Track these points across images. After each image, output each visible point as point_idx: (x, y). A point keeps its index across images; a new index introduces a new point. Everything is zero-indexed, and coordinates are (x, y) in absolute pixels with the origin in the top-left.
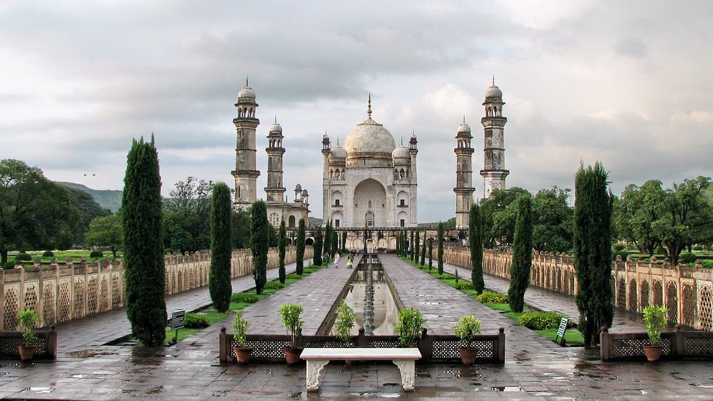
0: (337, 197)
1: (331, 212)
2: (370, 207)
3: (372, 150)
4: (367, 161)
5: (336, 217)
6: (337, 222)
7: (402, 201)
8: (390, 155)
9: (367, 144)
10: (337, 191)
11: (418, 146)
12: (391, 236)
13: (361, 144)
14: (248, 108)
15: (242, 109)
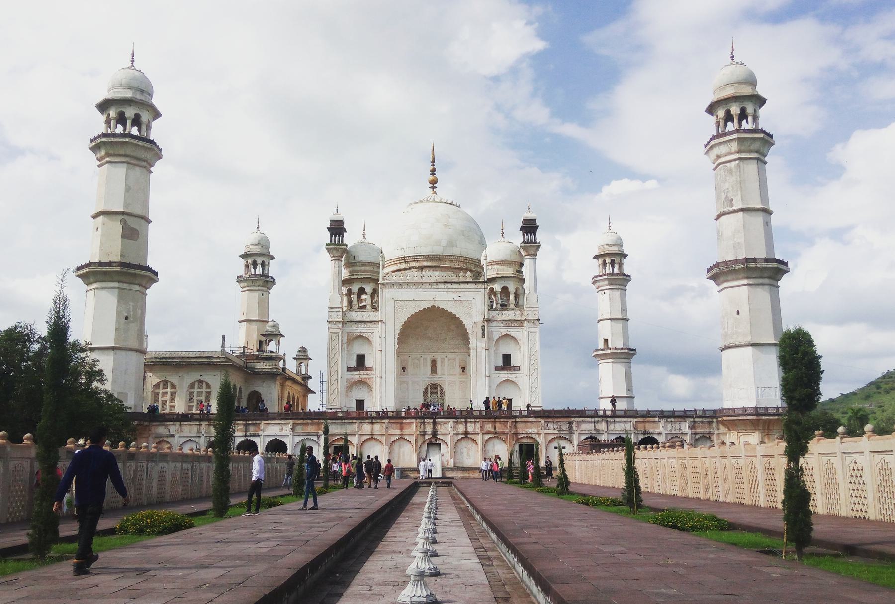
0: (359, 349)
2: (434, 370)
3: (438, 250)
4: (426, 273)
5: (359, 394)
7: (507, 358)
8: (477, 263)
10: (360, 336)
11: (540, 236)
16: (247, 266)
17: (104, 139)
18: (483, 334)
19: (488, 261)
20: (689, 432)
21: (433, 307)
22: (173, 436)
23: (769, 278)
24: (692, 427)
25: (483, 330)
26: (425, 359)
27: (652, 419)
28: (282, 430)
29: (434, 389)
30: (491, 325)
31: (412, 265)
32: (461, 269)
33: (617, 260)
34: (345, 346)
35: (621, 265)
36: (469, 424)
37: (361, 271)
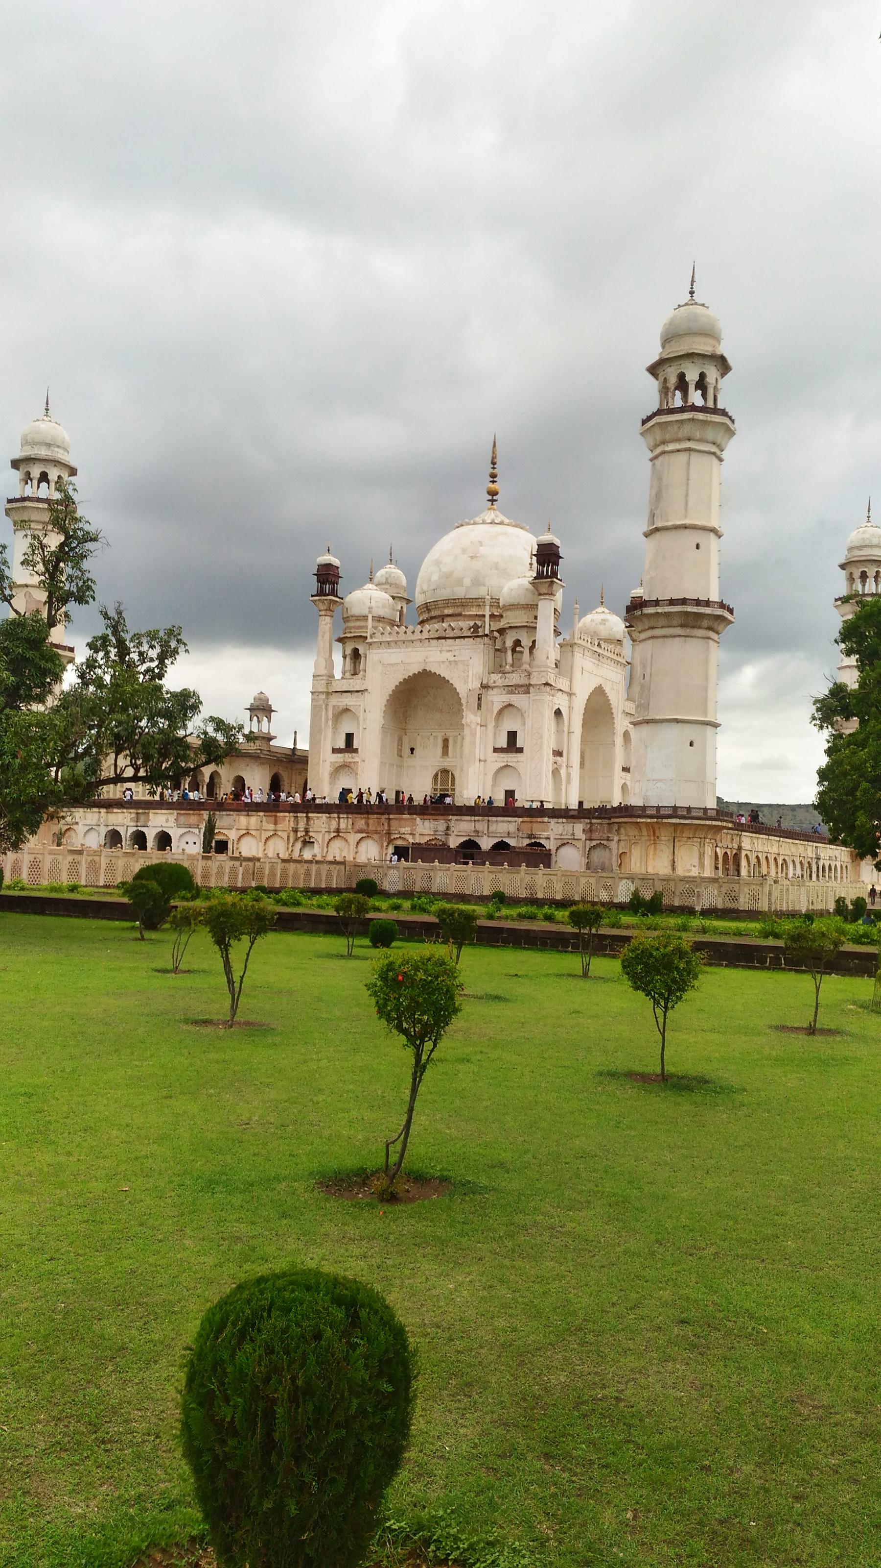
3: (460, 592)
6: (345, 792)
9: (448, 576)
12: (360, 831)
18: (479, 706)
20: (583, 837)
21: (425, 670)
22: (77, 823)
23: (682, 626)
24: (589, 831)
25: (479, 699)
26: (436, 737)
27: (539, 820)
28: (167, 821)
29: (445, 775)
30: (490, 692)
31: (433, 614)
34: (330, 723)
36: (342, 820)
37: (355, 627)
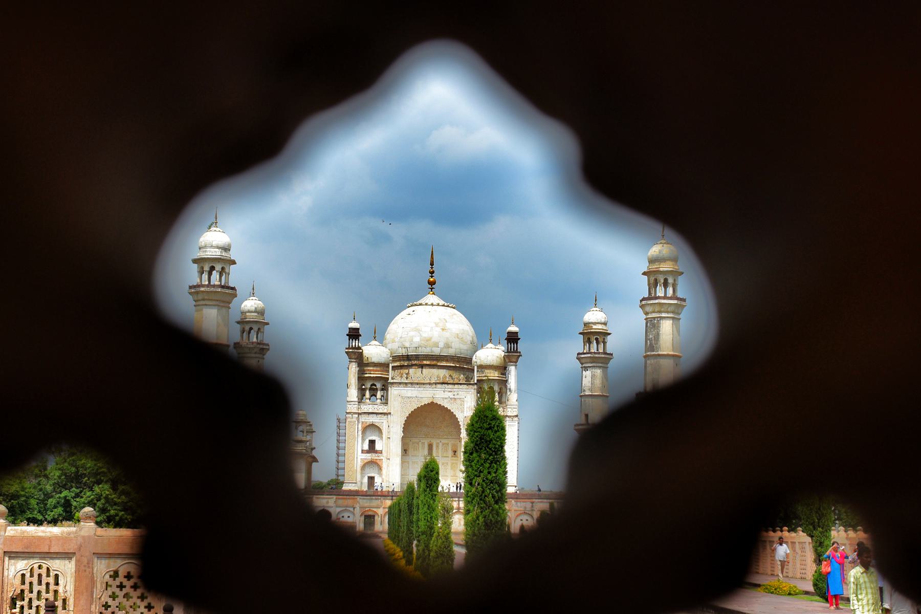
1: (359, 464)
3: (437, 351)
6: (371, 479)
8: (469, 361)
13: (417, 339)
14: (218, 267)
15: (207, 268)
16: (243, 331)
17: (202, 289)
19: (479, 363)
21: (432, 402)
26: (423, 443)
31: (414, 363)
32: (454, 368)
33: (600, 339)
34: (360, 433)
35: (604, 343)
